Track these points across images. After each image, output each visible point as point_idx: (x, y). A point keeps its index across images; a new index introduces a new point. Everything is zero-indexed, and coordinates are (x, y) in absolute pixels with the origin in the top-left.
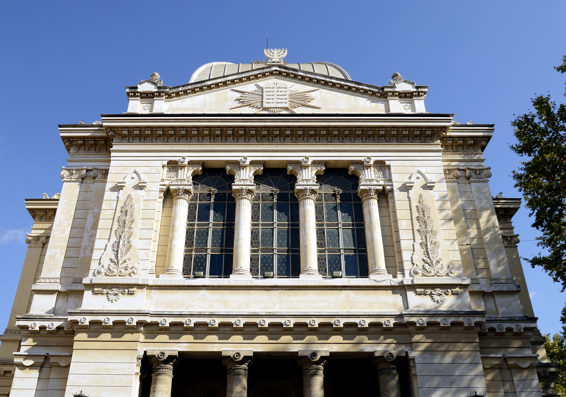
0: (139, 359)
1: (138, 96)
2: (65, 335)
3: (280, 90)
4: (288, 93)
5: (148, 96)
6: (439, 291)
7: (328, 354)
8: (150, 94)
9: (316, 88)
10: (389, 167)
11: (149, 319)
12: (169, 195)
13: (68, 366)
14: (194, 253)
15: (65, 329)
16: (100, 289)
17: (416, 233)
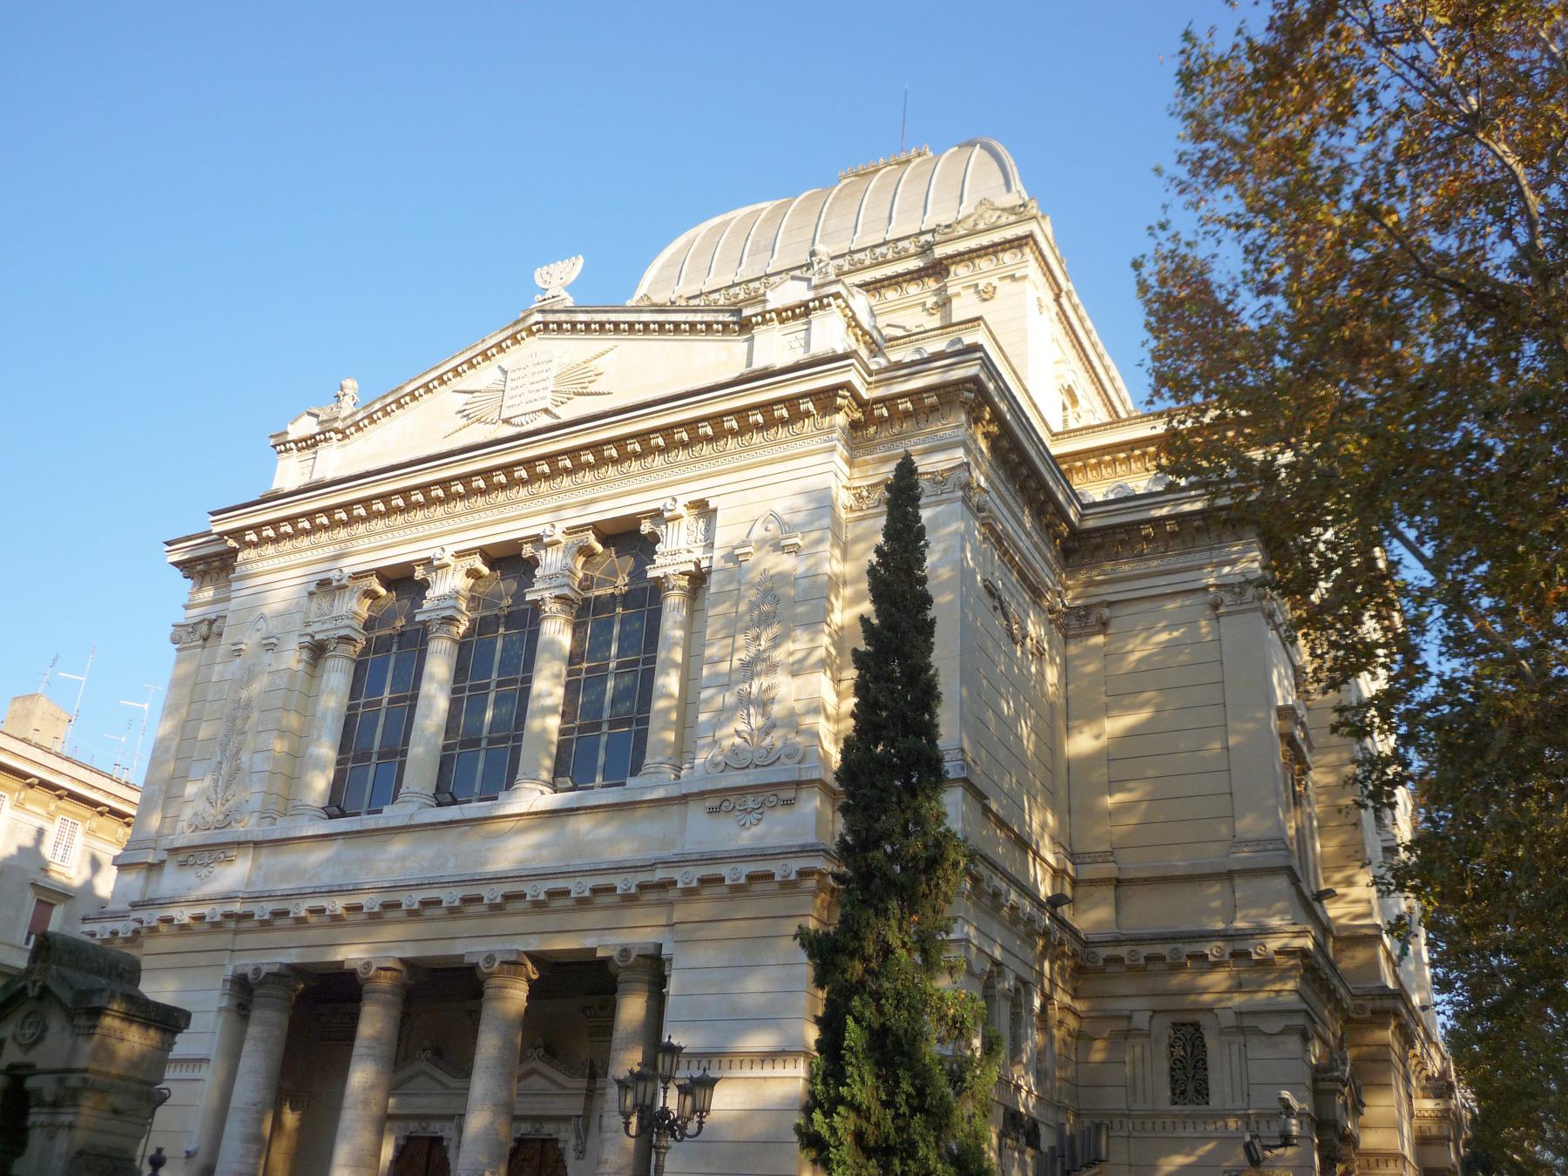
3: (538, 368)
9: (611, 344)
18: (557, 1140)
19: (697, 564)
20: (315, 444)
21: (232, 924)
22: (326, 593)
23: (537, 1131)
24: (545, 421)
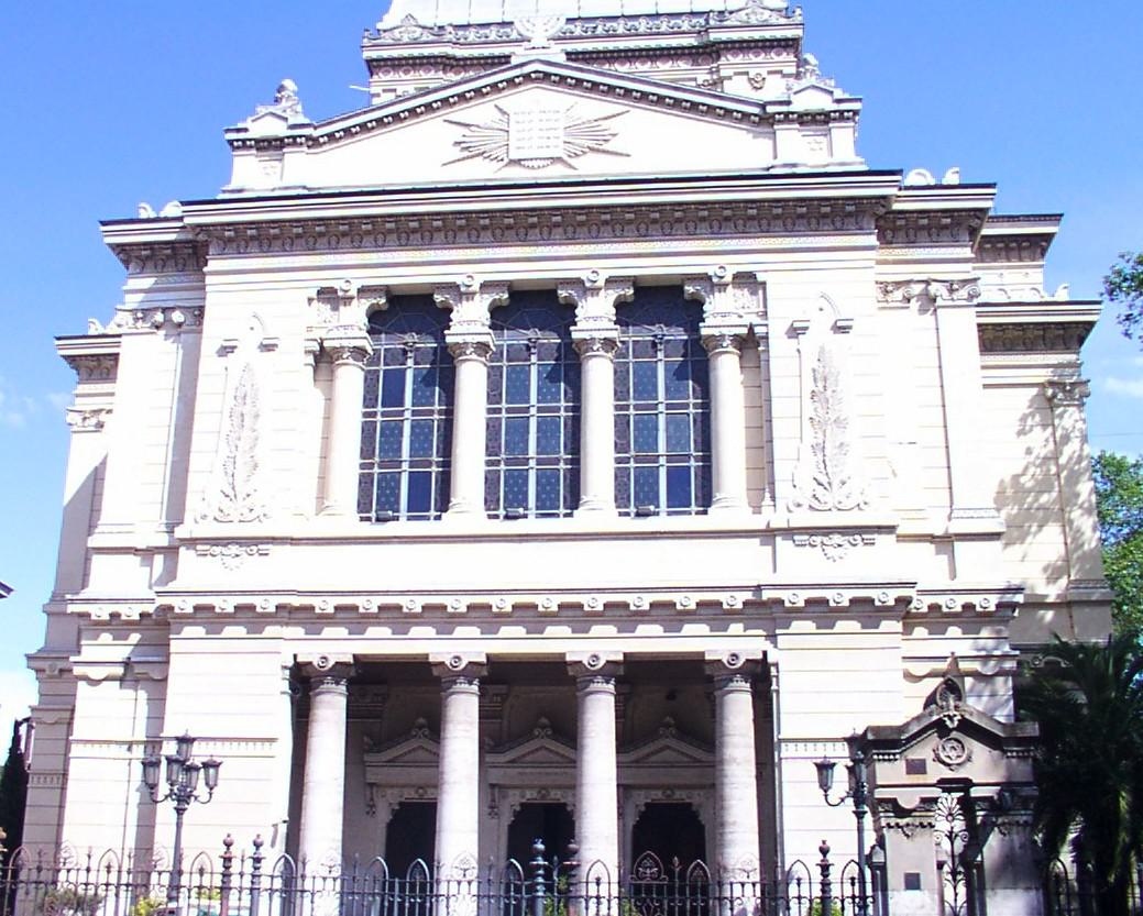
1: (251, 147)
2: (159, 627)
3: (544, 116)
4: (562, 124)
5: (271, 146)
6: (837, 539)
7: (621, 658)
8: (276, 140)
9: (621, 109)
10: (764, 283)
11: (296, 601)
12: (324, 359)
13: (165, 680)
14: (376, 470)
15: (154, 617)
16: (208, 547)
17: (806, 423)
19: (751, 328)
20: (282, 147)
22: (327, 301)
23: (543, 797)
24: (556, 173)
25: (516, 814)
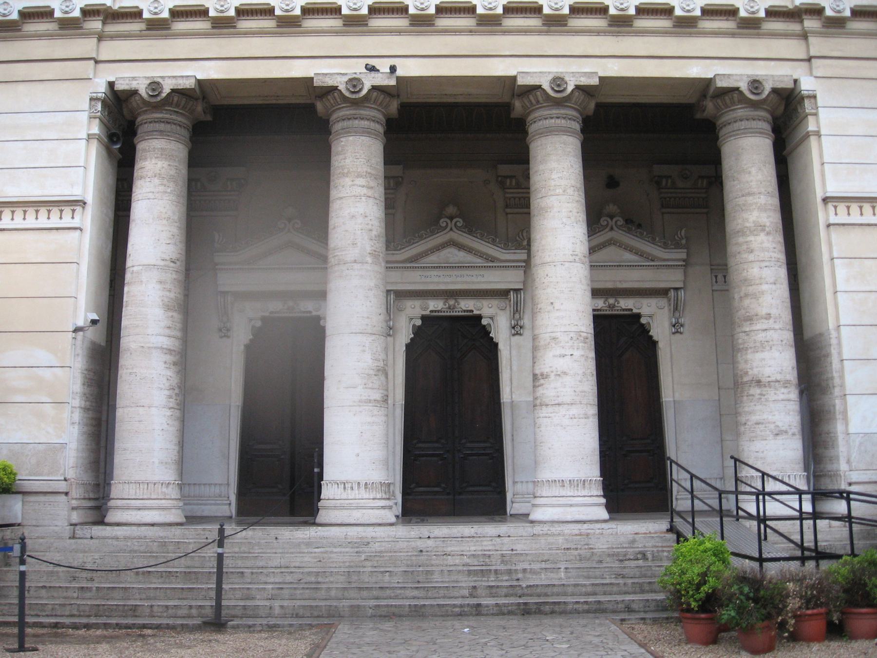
0: (97, 99)
7: (595, 81)
18: (479, 317)
21: (96, 25)
25: (418, 332)
